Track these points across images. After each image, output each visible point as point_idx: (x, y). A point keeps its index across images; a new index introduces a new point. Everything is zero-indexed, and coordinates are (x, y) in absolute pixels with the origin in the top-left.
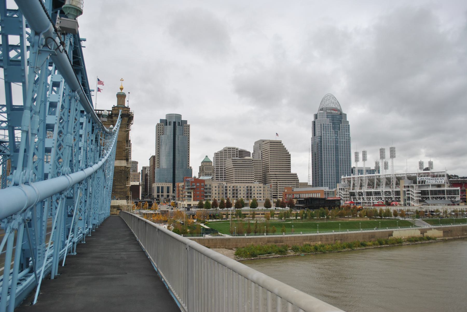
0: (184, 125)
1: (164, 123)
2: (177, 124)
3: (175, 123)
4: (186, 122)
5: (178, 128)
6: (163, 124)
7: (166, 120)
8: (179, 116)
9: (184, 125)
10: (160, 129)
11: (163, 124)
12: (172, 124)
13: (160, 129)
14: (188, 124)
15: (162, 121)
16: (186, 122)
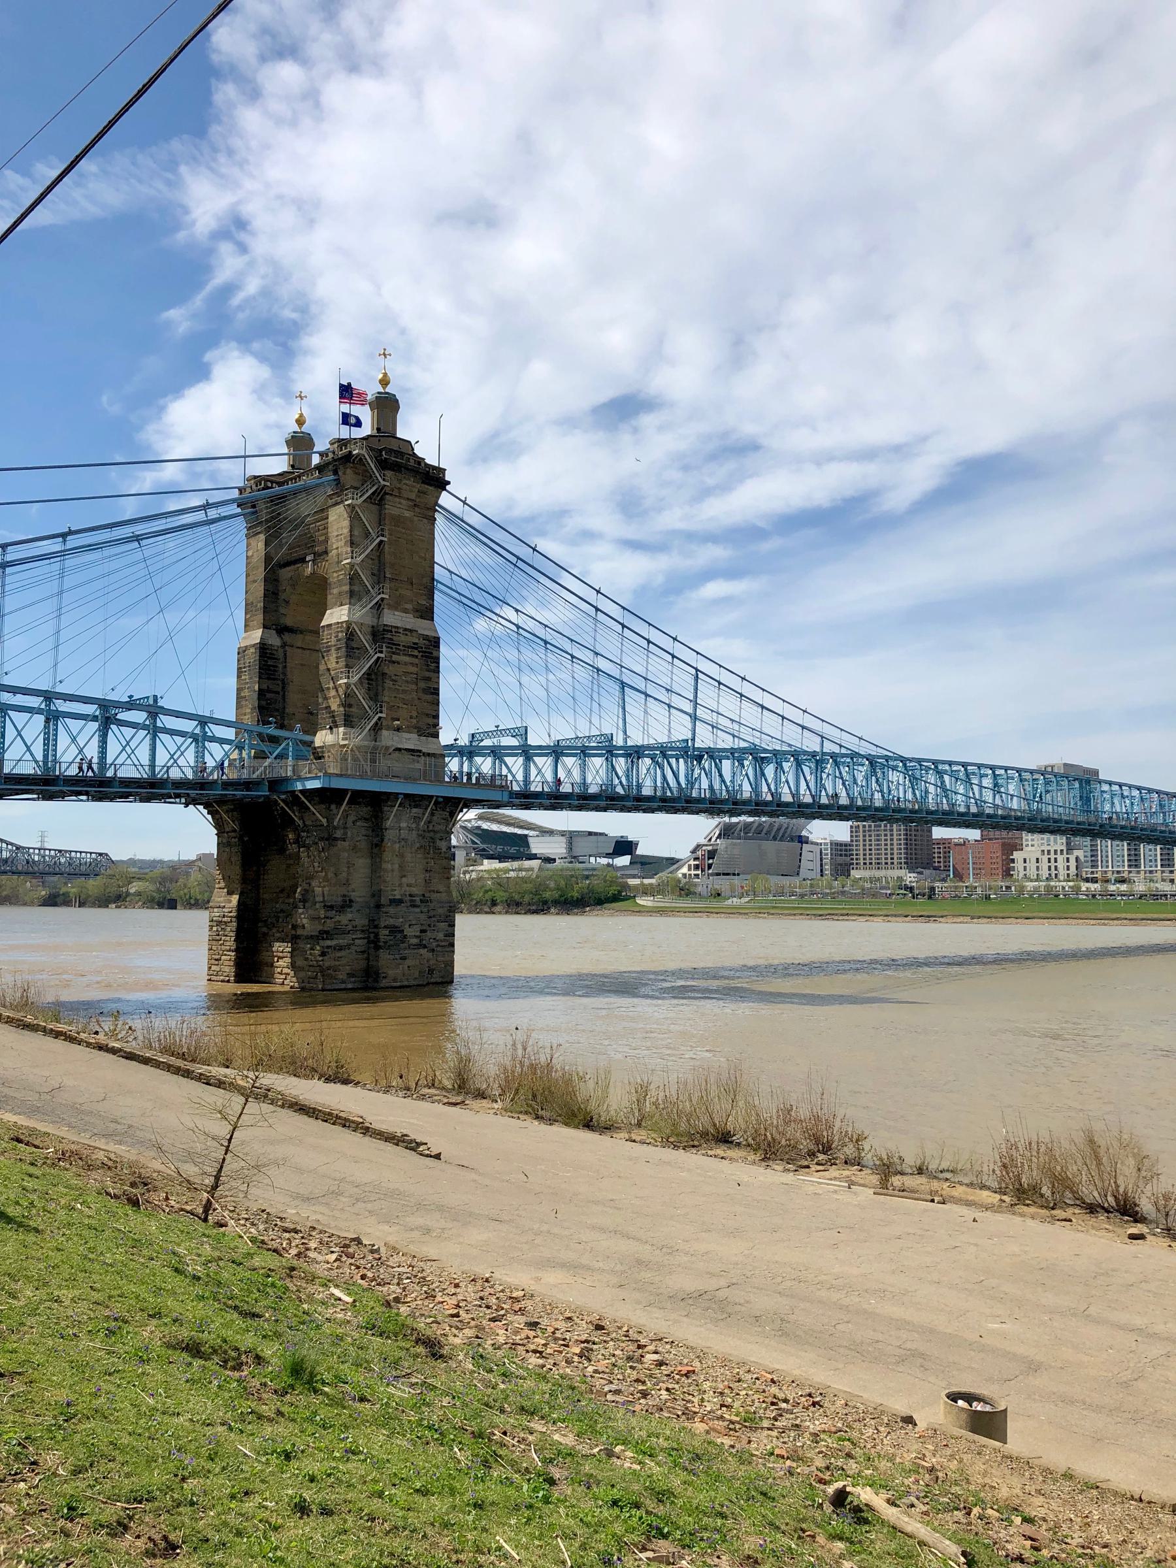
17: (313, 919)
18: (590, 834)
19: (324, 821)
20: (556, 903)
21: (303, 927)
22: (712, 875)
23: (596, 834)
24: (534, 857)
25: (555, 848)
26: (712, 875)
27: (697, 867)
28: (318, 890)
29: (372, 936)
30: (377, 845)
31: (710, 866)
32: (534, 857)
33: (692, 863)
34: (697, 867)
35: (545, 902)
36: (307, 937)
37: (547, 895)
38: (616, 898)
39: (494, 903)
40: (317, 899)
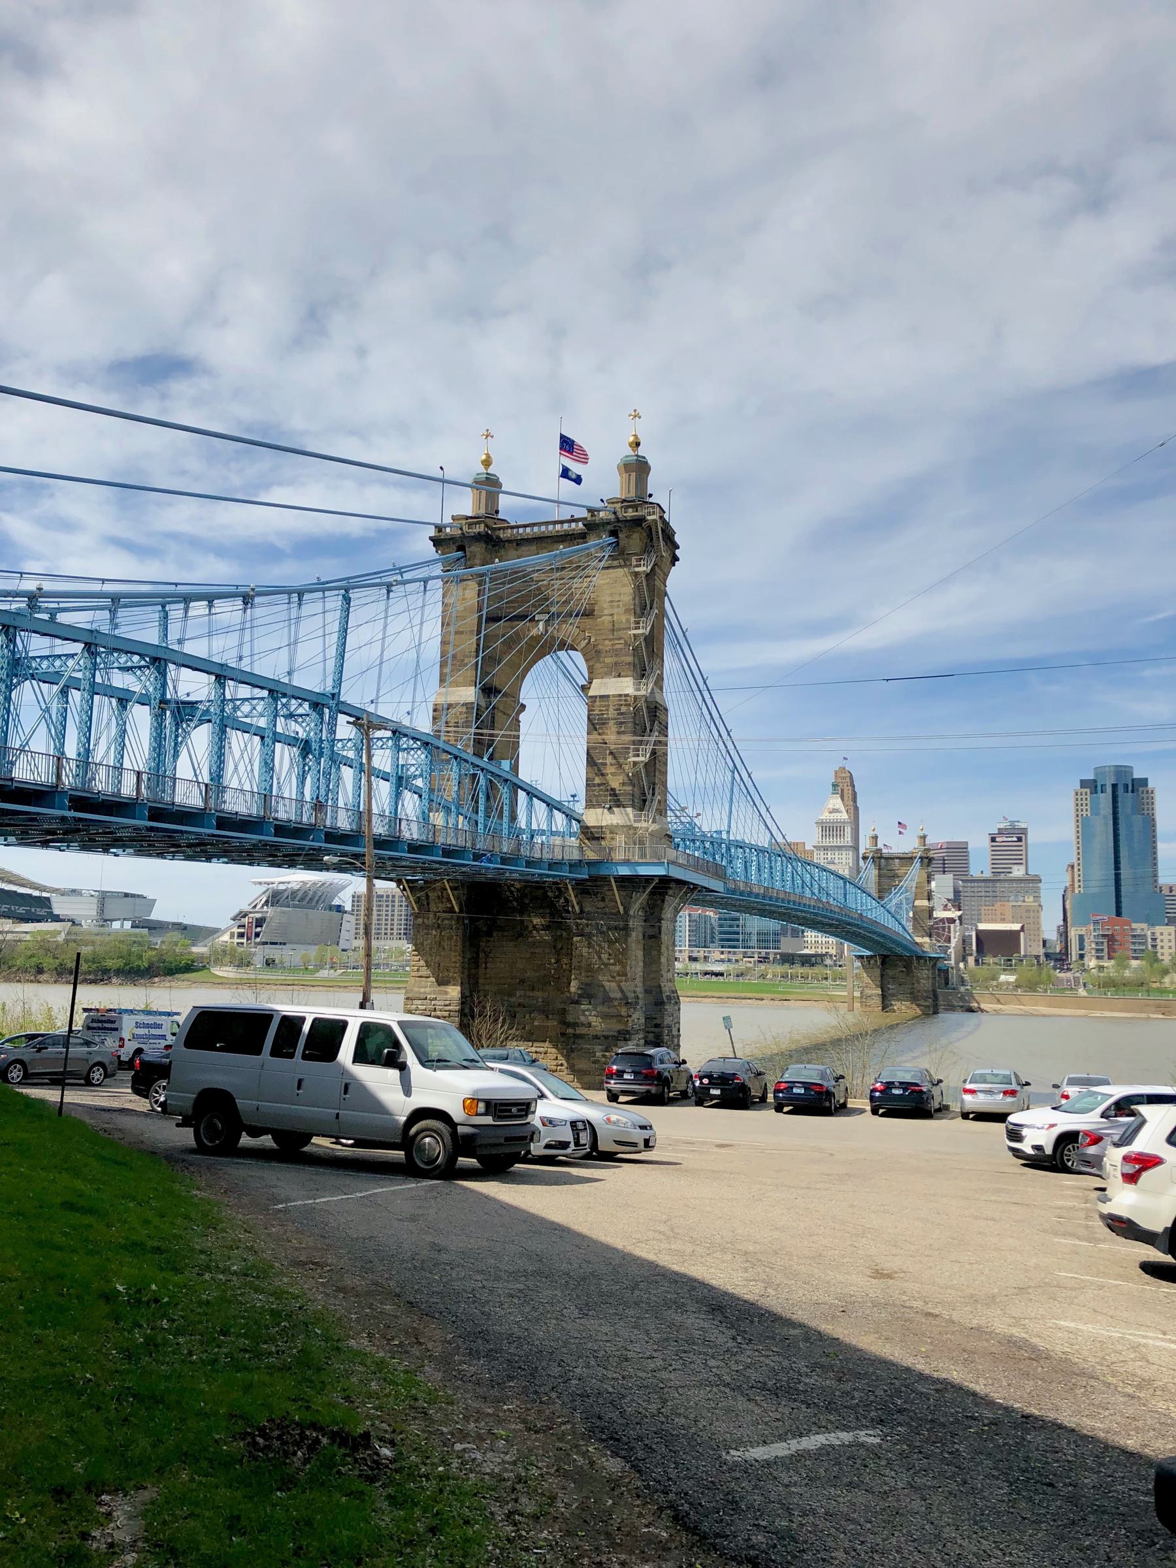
0: (1141, 789)
1: (1092, 786)
2: (1121, 789)
3: (1114, 786)
4: (1144, 782)
5: (1126, 799)
6: (1088, 790)
7: (1095, 781)
8: (1127, 770)
9: (1141, 789)
10: (1079, 802)
11: (1088, 790)
12: (1109, 789)
13: (1079, 802)
14: (1151, 785)
15: (1084, 784)
16: (1144, 782)
17: (605, 1016)
18: (126, 895)
19: (621, 909)
20: (119, 972)
21: (589, 1025)
22: (259, 944)
23: (133, 896)
24: (57, 919)
25: (85, 912)
26: (259, 944)
27: (241, 935)
28: (610, 986)
29: (651, 1037)
30: (652, 937)
31: (257, 935)
32: (57, 919)
33: (236, 930)
34: (241, 935)
35: (106, 971)
36: (596, 1037)
37: (109, 963)
38: (188, 968)
39: (40, 971)
40: (612, 995)
